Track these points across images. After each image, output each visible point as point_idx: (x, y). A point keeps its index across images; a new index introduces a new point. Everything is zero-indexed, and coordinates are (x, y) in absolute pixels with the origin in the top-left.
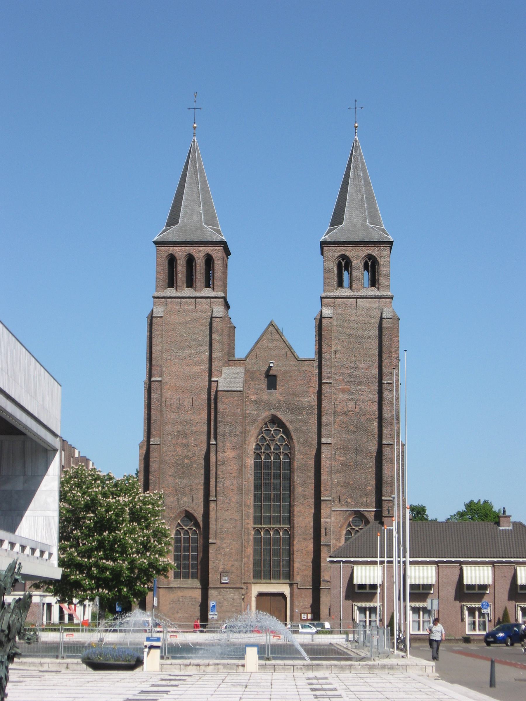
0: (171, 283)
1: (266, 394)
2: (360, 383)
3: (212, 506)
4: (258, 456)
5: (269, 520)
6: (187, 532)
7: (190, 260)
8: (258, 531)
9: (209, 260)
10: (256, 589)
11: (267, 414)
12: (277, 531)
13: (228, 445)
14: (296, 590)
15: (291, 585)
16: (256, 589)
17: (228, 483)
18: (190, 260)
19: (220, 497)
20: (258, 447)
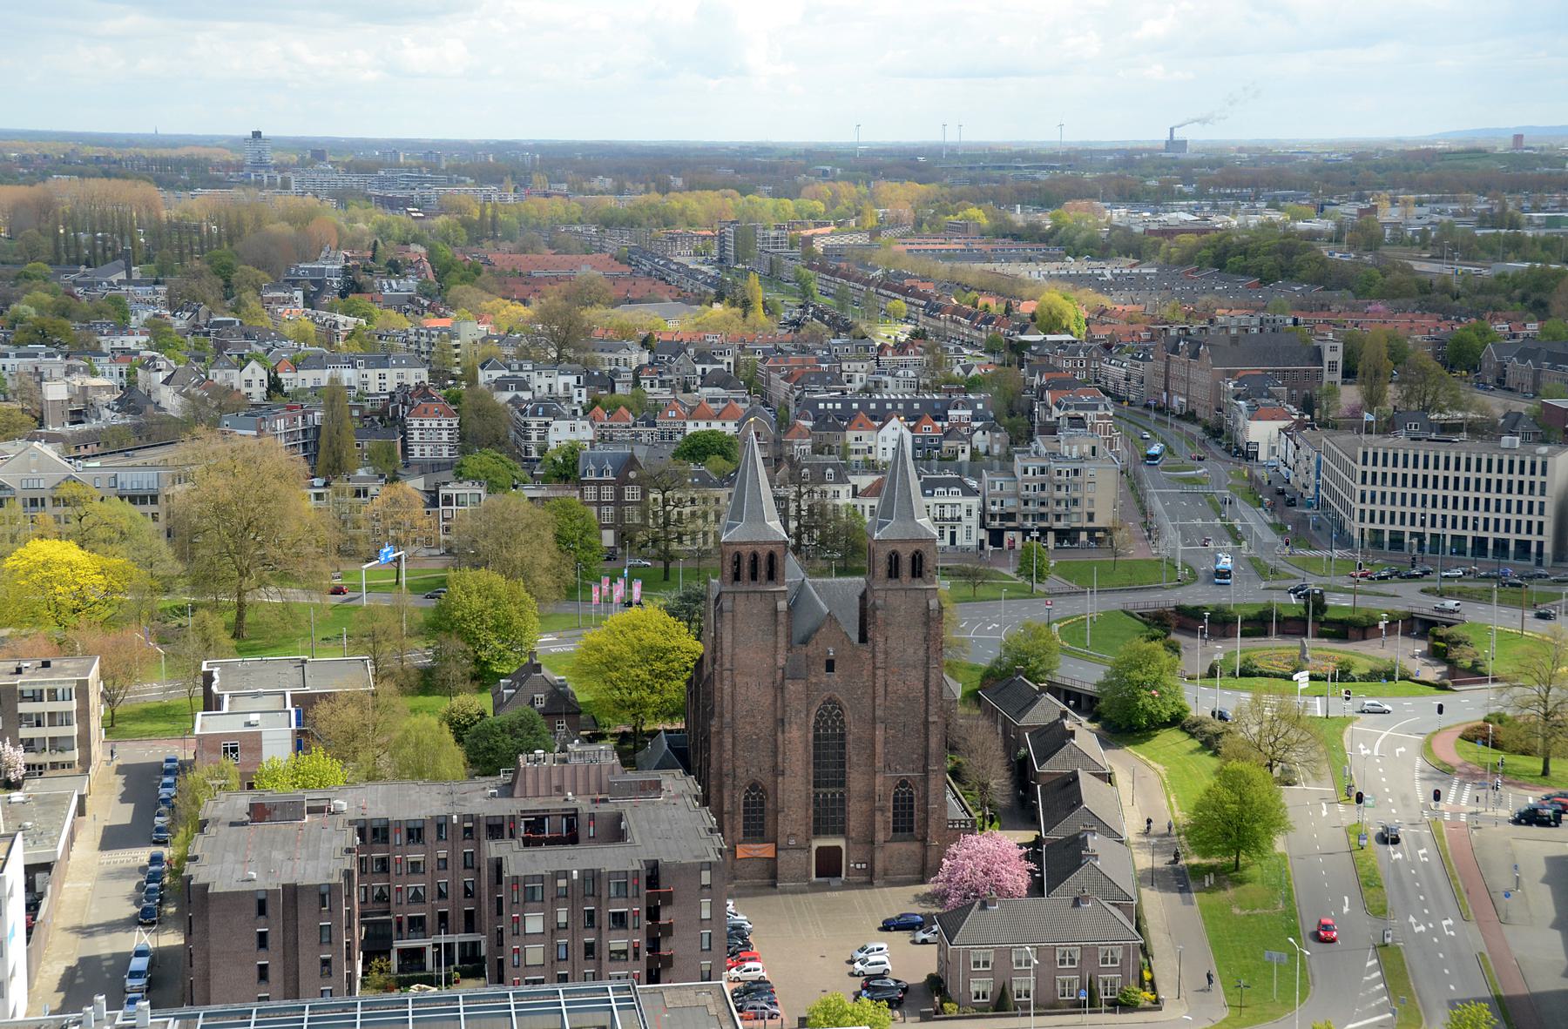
0: (737, 577)
1: (825, 677)
2: (908, 665)
3: (780, 779)
4: (817, 729)
5: (827, 785)
6: (754, 798)
7: (755, 556)
8: (817, 795)
9: (771, 556)
10: (816, 844)
11: (826, 695)
12: (833, 795)
13: (795, 727)
14: (851, 845)
15: (847, 839)
16: (816, 844)
17: (794, 759)
18: (755, 556)
19: (787, 772)
20: (817, 722)
